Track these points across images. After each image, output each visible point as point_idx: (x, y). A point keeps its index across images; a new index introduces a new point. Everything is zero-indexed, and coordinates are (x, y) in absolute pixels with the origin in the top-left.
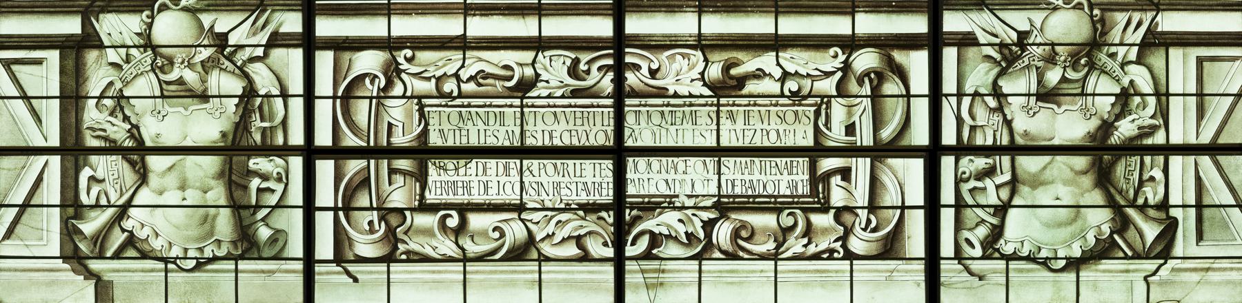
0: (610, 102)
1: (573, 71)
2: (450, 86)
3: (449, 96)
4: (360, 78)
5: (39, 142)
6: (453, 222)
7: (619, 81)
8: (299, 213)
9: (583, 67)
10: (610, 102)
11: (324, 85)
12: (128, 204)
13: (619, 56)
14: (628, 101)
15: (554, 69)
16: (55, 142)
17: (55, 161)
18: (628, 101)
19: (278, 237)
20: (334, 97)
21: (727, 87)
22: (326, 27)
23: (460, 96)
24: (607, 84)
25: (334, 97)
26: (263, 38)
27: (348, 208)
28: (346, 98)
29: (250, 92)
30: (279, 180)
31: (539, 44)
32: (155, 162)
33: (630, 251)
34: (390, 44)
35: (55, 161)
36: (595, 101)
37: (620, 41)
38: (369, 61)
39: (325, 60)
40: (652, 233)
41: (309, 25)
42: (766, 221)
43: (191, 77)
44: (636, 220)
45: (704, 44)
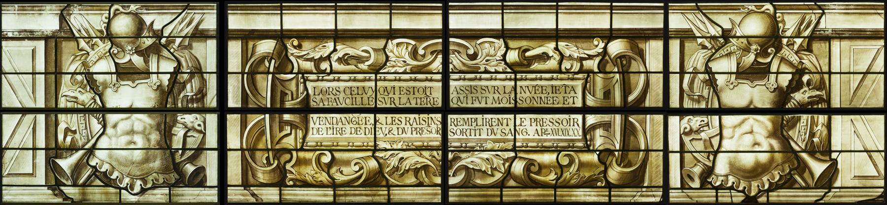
0: (439, 77)
1: (414, 54)
2: (324, 66)
3: (324, 72)
4: (262, 60)
5: (30, 104)
6: (326, 159)
7: (446, 62)
8: (215, 153)
9: (421, 52)
10: (439, 77)
11: (234, 63)
12: (94, 147)
13: (446, 44)
14: (453, 76)
15: (399, 52)
16: (41, 104)
17: (41, 118)
18: (453, 76)
19: (201, 170)
20: (243, 73)
21: (518, 69)
22: (236, 22)
23: (332, 72)
24: (437, 65)
25: (243, 73)
26: (189, 30)
27: (252, 150)
28: (251, 75)
29: (177, 71)
30: (200, 132)
31: (391, 34)
32: (112, 118)
33: (452, 181)
34: (281, 36)
35: (41, 118)
36: (429, 76)
37: (446, 33)
38: (266, 46)
39: (234, 48)
40: (466, 168)
41: (222, 20)
42: (548, 158)
43: (138, 61)
44: (456, 159)
45: (504, 34)
